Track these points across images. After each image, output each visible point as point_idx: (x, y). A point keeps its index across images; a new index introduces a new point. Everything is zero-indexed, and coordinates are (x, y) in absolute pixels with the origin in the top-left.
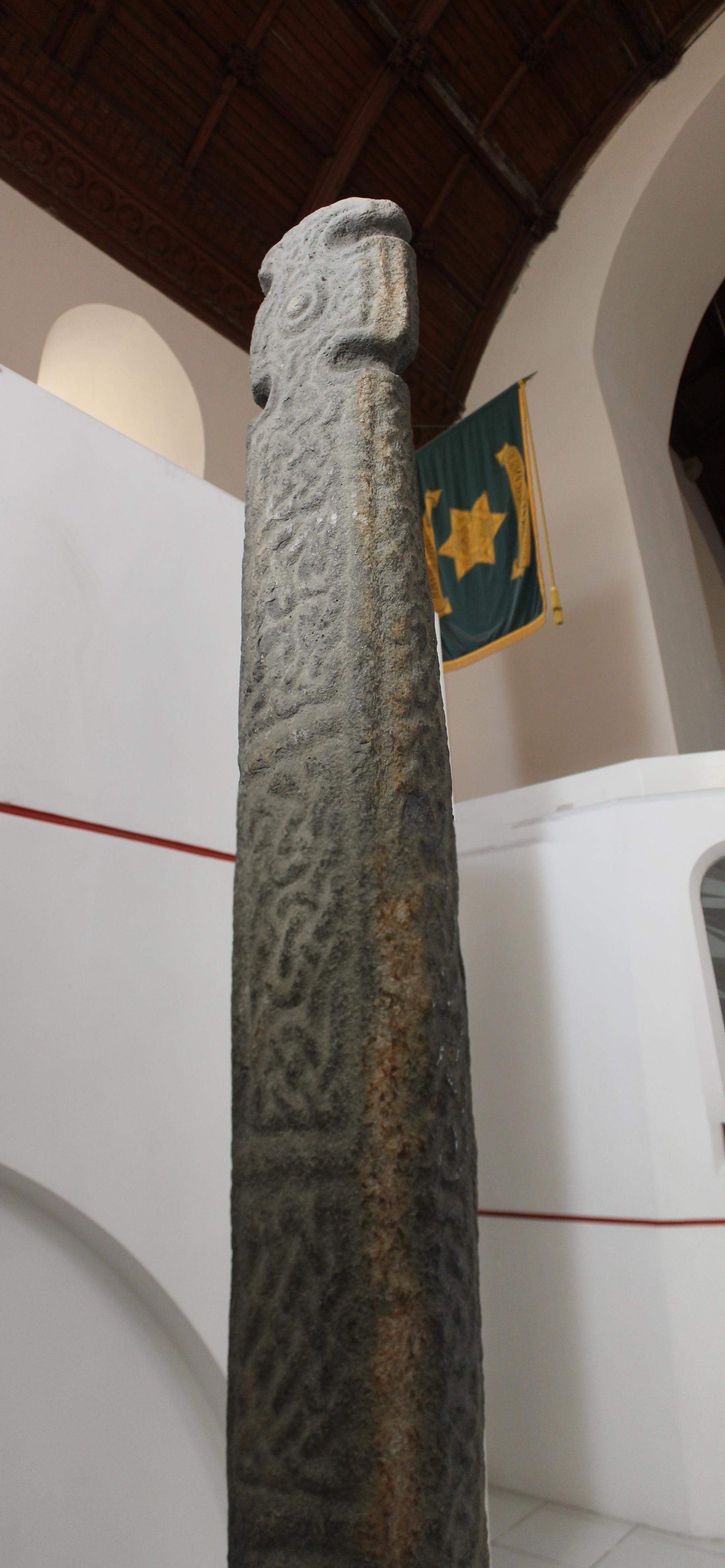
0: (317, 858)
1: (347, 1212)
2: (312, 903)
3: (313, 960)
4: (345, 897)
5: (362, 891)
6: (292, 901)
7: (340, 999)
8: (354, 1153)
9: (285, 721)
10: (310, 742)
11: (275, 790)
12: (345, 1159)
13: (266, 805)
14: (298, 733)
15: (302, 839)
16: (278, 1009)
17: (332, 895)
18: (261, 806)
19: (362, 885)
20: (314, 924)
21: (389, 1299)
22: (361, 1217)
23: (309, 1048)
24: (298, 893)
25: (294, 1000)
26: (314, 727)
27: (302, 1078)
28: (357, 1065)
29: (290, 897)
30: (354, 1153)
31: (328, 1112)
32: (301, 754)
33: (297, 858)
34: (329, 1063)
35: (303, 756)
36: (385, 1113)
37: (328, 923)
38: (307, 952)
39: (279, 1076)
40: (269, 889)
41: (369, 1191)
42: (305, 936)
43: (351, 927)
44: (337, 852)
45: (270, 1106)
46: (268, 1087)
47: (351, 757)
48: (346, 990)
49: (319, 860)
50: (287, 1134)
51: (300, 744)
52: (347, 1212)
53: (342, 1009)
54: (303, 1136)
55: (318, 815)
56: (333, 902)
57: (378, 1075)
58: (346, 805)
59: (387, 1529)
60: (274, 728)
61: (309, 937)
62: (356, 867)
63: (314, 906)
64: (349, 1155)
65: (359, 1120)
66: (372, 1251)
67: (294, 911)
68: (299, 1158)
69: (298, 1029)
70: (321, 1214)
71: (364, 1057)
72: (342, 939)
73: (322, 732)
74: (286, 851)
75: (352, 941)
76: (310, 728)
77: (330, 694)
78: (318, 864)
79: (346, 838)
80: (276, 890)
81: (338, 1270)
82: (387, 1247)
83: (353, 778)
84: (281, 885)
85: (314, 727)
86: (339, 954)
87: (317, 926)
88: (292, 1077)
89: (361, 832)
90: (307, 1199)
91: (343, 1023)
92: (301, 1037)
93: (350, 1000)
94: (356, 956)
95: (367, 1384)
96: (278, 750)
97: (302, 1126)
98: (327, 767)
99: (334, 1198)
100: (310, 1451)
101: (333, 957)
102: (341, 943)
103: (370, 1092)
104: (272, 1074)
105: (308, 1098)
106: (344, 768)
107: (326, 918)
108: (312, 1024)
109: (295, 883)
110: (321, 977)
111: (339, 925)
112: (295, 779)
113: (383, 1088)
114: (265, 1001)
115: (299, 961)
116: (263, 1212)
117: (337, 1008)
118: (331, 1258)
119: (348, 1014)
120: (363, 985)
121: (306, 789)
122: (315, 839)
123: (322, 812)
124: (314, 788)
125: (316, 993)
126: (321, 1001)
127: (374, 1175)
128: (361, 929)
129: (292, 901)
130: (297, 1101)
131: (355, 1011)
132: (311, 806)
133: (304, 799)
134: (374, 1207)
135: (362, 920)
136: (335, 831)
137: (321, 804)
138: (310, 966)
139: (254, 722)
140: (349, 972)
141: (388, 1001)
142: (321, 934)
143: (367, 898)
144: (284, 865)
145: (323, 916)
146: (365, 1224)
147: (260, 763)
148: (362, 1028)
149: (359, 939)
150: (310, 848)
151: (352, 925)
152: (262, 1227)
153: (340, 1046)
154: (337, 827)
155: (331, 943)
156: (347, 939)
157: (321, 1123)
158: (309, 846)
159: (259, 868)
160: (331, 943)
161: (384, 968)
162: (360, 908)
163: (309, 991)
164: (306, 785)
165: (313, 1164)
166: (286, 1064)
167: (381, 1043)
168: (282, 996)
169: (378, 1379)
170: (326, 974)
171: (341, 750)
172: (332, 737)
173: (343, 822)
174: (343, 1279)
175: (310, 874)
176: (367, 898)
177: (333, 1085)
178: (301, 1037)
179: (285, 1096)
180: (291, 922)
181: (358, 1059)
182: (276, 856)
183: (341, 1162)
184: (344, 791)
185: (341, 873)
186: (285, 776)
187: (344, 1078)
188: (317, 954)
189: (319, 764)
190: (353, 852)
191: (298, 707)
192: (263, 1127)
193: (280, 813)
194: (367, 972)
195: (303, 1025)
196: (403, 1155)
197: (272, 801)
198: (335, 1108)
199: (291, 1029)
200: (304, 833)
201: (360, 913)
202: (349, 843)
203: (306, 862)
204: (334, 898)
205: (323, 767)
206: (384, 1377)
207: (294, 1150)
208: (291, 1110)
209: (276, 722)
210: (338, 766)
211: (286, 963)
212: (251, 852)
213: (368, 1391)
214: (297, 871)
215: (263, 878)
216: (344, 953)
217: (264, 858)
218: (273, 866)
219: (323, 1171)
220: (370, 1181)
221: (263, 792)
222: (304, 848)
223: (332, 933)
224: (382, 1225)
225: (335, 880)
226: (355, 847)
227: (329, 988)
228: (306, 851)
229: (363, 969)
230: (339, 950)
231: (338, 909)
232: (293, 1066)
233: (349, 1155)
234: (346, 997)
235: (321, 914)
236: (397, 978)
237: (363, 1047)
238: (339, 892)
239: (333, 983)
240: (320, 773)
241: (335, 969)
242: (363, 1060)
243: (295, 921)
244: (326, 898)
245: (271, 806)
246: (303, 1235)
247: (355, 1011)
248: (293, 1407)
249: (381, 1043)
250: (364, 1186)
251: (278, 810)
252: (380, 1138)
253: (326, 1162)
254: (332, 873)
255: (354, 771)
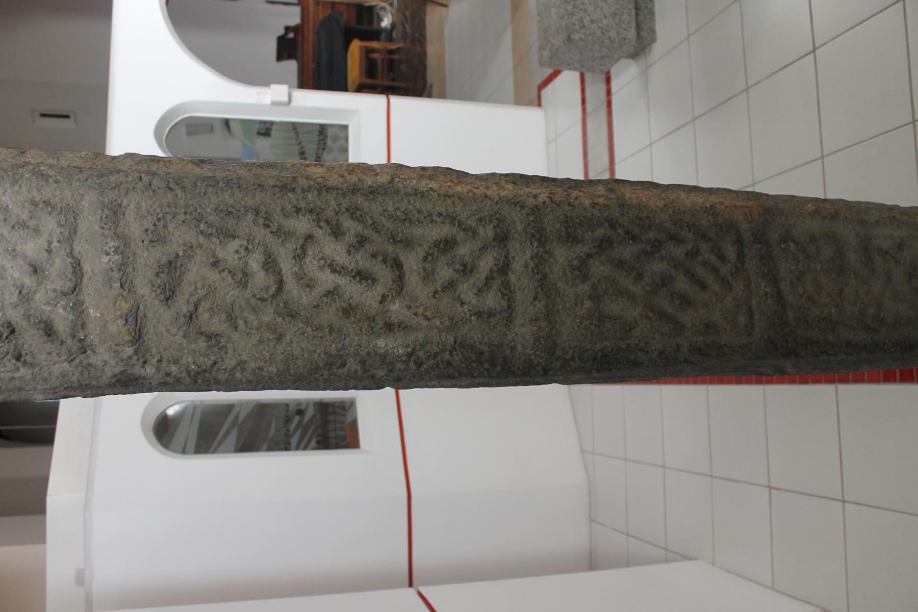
0: (261, 233)
1: (566, 216)
2: (306, 241)
3: (362, 241)
4: (303, 205)
5: (298, 190)
6: (301, 267)
7: (398, 213)
8: (522, 207)
9: (85, 280)
10: (125, 240)
11: (169, 296)
12: (528, 214)
13: (185, 310)
14: (108, 254)
15: (237, 252)
16: (404, 291)
17: (300, 217)
18: (185, 317)
19: (293, 190)
20: (328, 238)
21: (614, 196)
22: (566, 207)
23: (442, 245)
24: (294, 258)
25: (398, 265)
26: (106, 232)
27: (467, 258)
28: (453, 202)
29: (296, 269)
30: (522, 207)
31: (495, 227)
32: (134, 254)
33: (255, 263)
34: (454, 225)
35: (138, 252)
36: (487, 188)
37: (328, 222)
38: (354, 247)
39: (466, 289)
40: (282, 305)
41: (548, 201)
42: (337, 251)
43: (333, 203)
44: (257, 212)
45: (492, 300)
46: (474, 302)
47: (154, 191)
48: (390, 209)
49: (263, 232)
50: (512, 278)
51: (122, 253)
52: (566, 216)
53: (408, 212)
54: (513, 258)
55: (214, 231)
56: (308, 216)
57: (459, 189)
58: (207, 202)
59: (743, 207)
60: (88, 301)
61: (338, 247)
62: (275, 194)
63: (309, 237)
64: (525, 212)
65: (497, 203)
66: (587, 202)
67: (311, 265)
68: (532, 258)
69: (425, 259)
70: (570, 238)
71: (447, 196)
72: (344, 210)
73: (116, 223)
74: (244, 279)
75: (345, 203)
76: (106, 238)
77: (69, 216)
78: (268, 230)
79: (243, 203)
80: (284, 296)
81: (607, 225)
82: (581, 194)
83: (178, 192)
84: (280, 284)
85: (106, 232)
86: (358, 212)
87: (330, 235)
88: (467, 270)
89: (239, 187)
90: (562, 255)
91: (419, 212)
92: (432, 255)
93: (399, 205)
94: (360, 200)
95: (670, 212)
96: (122, 286)
97: (506, 257)
98: (161, 216)
99: (558, 226)
100: (722, 258)
101: (360, 220)
102: (347, 210)
103: (474, 194)
104: (463, 296)
105: (484, 248)
106: (165, 201)
107: (322, 224)
108: (420, 245)
109: (282, 265)
110: (378, 232)
111: (330, 213)
112: (164, 260)
113: (469, 187)
114: (396, 307)
115: (361, 260)
116: (577, 305)
117: (407, 219)
118: (600, 232)
119: (411, 207)
120: (386, 194)
121: (180, 245)
122: (238, 237)
123: (210, 225)
124: (180, 236)
125: (393, 239)
126: (400, 235)
127: (535, 196)
128: (334, 193)
129: (301, 267)
130: (486, 264)
131: (409, 201)
132: (201, 239)
133: (191, 247)
134: (557, 198)
135: (327, 190)
136: (235, 212)
137: (202, 226)
138: (367, 246)
139: (69, 341)
140: (374, 208)
141: (397, 179)
142: (337, 233)
143: (305, 187)
144: (261, 279)
145: (321, 227)
146: (570, 205)
147: (130, 320)
148: (423, 196)
149: (344, 195)
150: (248, 240)
151: (331, 203)
152: (588, 304)
153: (440, 215)
154: (230, 209)
155: (347, 223)
156: (344, 205)
157: (502, 238)
158: (245, 242)
159: (256, 322)
160: (347, 223)
161: (369, 181)
162: (316, 192)
163: (390, 248)
164: (175, 246)
165: (536, 244)
166: (456, 276)
167: (433, 185)
168: (394, 281)
169: (665, 206)
170: (375, 227)
171: (143, 203)
172: (124, 214)
173: (226, 205)
174: (613, 224)
175: (274, 244)
176: (305, 187)
177: (472, 222)
178: (432, 255)
179: (483, 276)
180: (321, 268)
181: (449, 201)
182: (247, 294)
183: (531, 218)
184: (191, 202)
185: (279, 209)
186: (157, 275)
187: (466, 214)
188: (357, 236)
189: (155, 225)
190: (259, 196)
191: (73, 258)
192: (509, 307)
193: (199, 285)
194: (374, 192)
195: (420, 252)
196: (515, 183)
197: (182, 304)
198: (491, 221)
199: (424, 269)
200: (229, 252)
201: (320, 193)
202: (250, 202)
203: (261, 249)
204: (304, 215)
205: (159, 220)
206: (662, 202)
207: (526, 266)
208: (495, 268)
209: (81, 298)
210: (161, 206)
211: (362, 276)
212: (235, 336)
213: (674, 212)
214: (270, 264)
215: (268, 315)
216: (357, 209)
217: (246, 314)
218: (258, 296)
219: (539, 235)
220: (540, 199)
221: (167, 315)
222: (247, 249)
223: (338, 220)
224: (568, 195)
225: (286, 214)
226: (254, 194)
227: (389, 225)
228: (250, 247)
229: (372, 193)
230: (355, 213)
231: (316, 214)
232: (457, 267)
233: (525, 212)
234: (397, 209)
235: (319, 230)
236: (377, 174)
237: (439, 196)
238: (298, 210)
239: (384, 221)
240: (165, 227)
241: (371, 217)
242: (449, 196)
243: (322, 262)
244: (302, 225)
245: (188, 302)
246: (589, 256)
247: (409, 201)
248: (700, 271)
249: (433, 185)
250: (544, 202)
251: (196, 288)
252: (506, 192)
253: (532, 231)
254: (278, 218)
255: (171, 189)
